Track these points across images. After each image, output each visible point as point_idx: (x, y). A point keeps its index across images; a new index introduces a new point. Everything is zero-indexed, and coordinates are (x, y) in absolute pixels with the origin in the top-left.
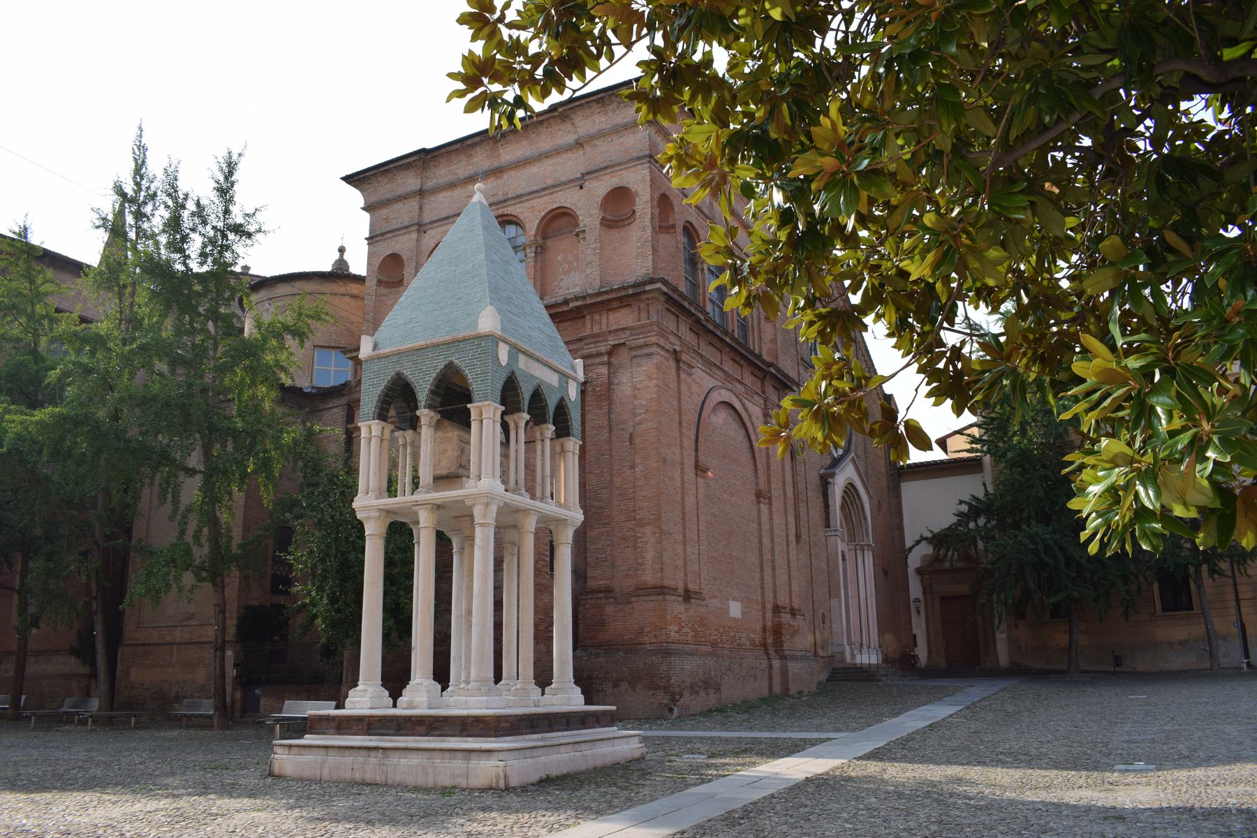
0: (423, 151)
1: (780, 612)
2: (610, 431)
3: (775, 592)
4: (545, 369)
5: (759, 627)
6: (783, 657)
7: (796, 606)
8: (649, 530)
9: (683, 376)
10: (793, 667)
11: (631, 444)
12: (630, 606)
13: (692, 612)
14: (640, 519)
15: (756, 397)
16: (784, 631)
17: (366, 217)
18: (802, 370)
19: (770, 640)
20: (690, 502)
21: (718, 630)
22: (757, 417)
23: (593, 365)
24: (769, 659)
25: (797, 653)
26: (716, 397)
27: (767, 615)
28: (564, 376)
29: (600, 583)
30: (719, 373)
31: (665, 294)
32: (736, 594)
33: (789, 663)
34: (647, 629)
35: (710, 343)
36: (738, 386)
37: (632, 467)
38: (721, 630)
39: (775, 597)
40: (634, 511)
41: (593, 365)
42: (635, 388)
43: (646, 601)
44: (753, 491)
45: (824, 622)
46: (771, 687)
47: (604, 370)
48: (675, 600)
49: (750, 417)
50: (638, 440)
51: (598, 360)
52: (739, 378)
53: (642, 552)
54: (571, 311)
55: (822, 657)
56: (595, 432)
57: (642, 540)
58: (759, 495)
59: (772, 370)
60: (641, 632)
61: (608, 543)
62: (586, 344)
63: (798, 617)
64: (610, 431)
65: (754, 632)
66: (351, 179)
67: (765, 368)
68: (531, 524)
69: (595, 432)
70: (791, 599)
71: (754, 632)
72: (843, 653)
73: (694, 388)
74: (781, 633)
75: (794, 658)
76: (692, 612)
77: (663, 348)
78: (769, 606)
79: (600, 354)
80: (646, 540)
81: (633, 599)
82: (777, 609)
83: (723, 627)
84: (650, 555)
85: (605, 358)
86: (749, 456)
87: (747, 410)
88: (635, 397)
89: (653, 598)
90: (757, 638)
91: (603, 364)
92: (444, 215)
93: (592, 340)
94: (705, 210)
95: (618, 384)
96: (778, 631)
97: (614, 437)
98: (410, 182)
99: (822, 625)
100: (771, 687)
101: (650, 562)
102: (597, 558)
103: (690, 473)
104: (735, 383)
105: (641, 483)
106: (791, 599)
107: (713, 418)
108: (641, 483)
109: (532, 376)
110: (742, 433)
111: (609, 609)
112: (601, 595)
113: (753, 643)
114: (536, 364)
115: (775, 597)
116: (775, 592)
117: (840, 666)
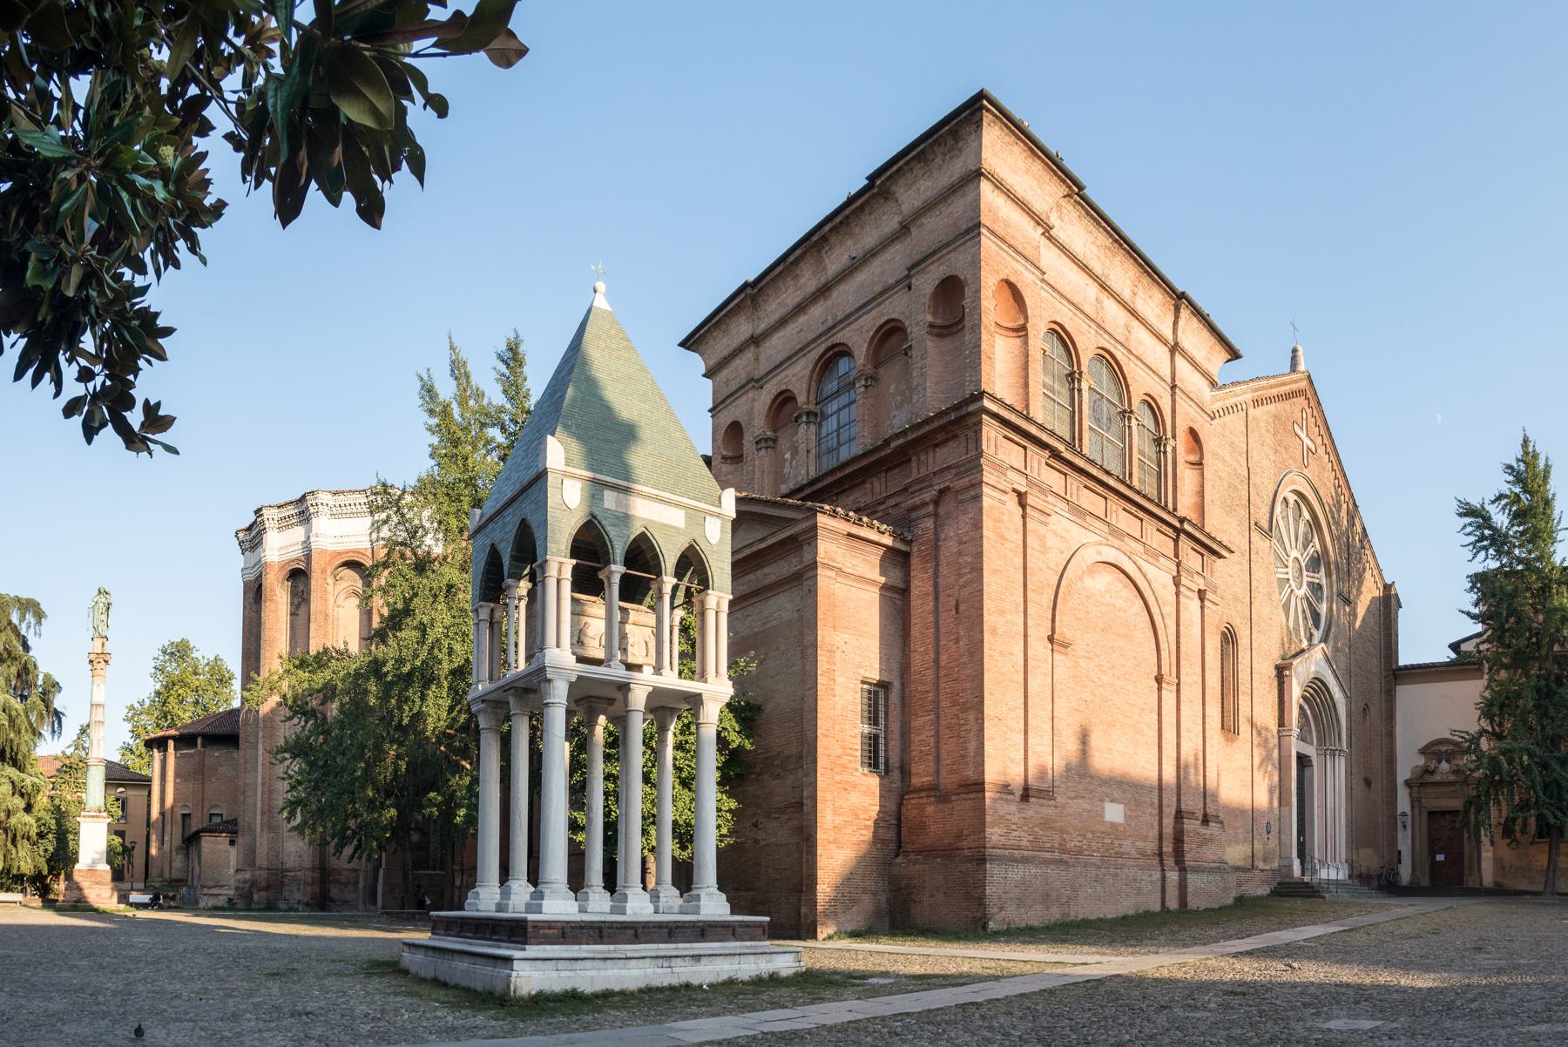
1: (1182, 818)
2: (937, 599)
3: (1179, 795)
5: (1154, 833)
6: (1183, 870)
7: (1211, 810)
8: (971, 716)
9: (1031, 525)
10: (1194, 880)
11: (957, 613)
12: (950, 805)
13: (1030, 813)
14: (964, 703)
16: (1186, 839)
19: (1168, 848)
20: (1038, 682)
23: (918, 518)
24: (1163, 870)
25: (1205, 864)
26: (1090, 555)
27: (1165, 821)
29: (924, 779)
30: (1098, 524)
33: (1189, 876)
34: (965, 833)
37: (957, 641)
38: (1089, 835)
39: (1179, 800)
40: (958, 695)
41: (918, 518)
42: (961, 543)
43: (965, 800)
45: (1268, 833)
46: (1163, 902)
47: (929, 523)
50: (962, 607)
51: (923, 512)
53: (965, 742)
54: (895, 453)
55: (1262, 871)
56: (920, 602)
57: (965, 727)
58: (1159, 679)
60: (959, 836)
61: (932, 733)
62: (912, 493)
63: (1211, 824)
64: (937, 599)
65: (1145, 839)
69: (920, 602)
70: (1205, 804)
72: (1290, 867)
73: (1051, 542)
74: (1183, 841)
75: (1196, 870)
76: (1030, 813)
78: (1170, 811)
79: (925, 504)
80: (968, 727)
81: (953, 798)
82: (1179, 815)
83: (1093, 832)
84: (972, 746)
85: (931, 508)
88: (960, 553)
89: (972, 796)
90: (1151, 846)
91: (928, 515)
92: (778, 362)
93: (917, 487)
95: (945, 540)
96: (1178, 840)
97: (940, 606)
99: (1265, 835)
100: (1163, 902)
101: (972, 754)
102: (921, 752)
103: (1039, 647)
105: (965, 659)
106: (1205, 804)
107: (1088, 581)
108: (965, 659)
111: (930, 810)
112: (923, 794)
113: (1143, 854)
115: (1179, 800)
116: (1179, 795)
117: (1287, 880)
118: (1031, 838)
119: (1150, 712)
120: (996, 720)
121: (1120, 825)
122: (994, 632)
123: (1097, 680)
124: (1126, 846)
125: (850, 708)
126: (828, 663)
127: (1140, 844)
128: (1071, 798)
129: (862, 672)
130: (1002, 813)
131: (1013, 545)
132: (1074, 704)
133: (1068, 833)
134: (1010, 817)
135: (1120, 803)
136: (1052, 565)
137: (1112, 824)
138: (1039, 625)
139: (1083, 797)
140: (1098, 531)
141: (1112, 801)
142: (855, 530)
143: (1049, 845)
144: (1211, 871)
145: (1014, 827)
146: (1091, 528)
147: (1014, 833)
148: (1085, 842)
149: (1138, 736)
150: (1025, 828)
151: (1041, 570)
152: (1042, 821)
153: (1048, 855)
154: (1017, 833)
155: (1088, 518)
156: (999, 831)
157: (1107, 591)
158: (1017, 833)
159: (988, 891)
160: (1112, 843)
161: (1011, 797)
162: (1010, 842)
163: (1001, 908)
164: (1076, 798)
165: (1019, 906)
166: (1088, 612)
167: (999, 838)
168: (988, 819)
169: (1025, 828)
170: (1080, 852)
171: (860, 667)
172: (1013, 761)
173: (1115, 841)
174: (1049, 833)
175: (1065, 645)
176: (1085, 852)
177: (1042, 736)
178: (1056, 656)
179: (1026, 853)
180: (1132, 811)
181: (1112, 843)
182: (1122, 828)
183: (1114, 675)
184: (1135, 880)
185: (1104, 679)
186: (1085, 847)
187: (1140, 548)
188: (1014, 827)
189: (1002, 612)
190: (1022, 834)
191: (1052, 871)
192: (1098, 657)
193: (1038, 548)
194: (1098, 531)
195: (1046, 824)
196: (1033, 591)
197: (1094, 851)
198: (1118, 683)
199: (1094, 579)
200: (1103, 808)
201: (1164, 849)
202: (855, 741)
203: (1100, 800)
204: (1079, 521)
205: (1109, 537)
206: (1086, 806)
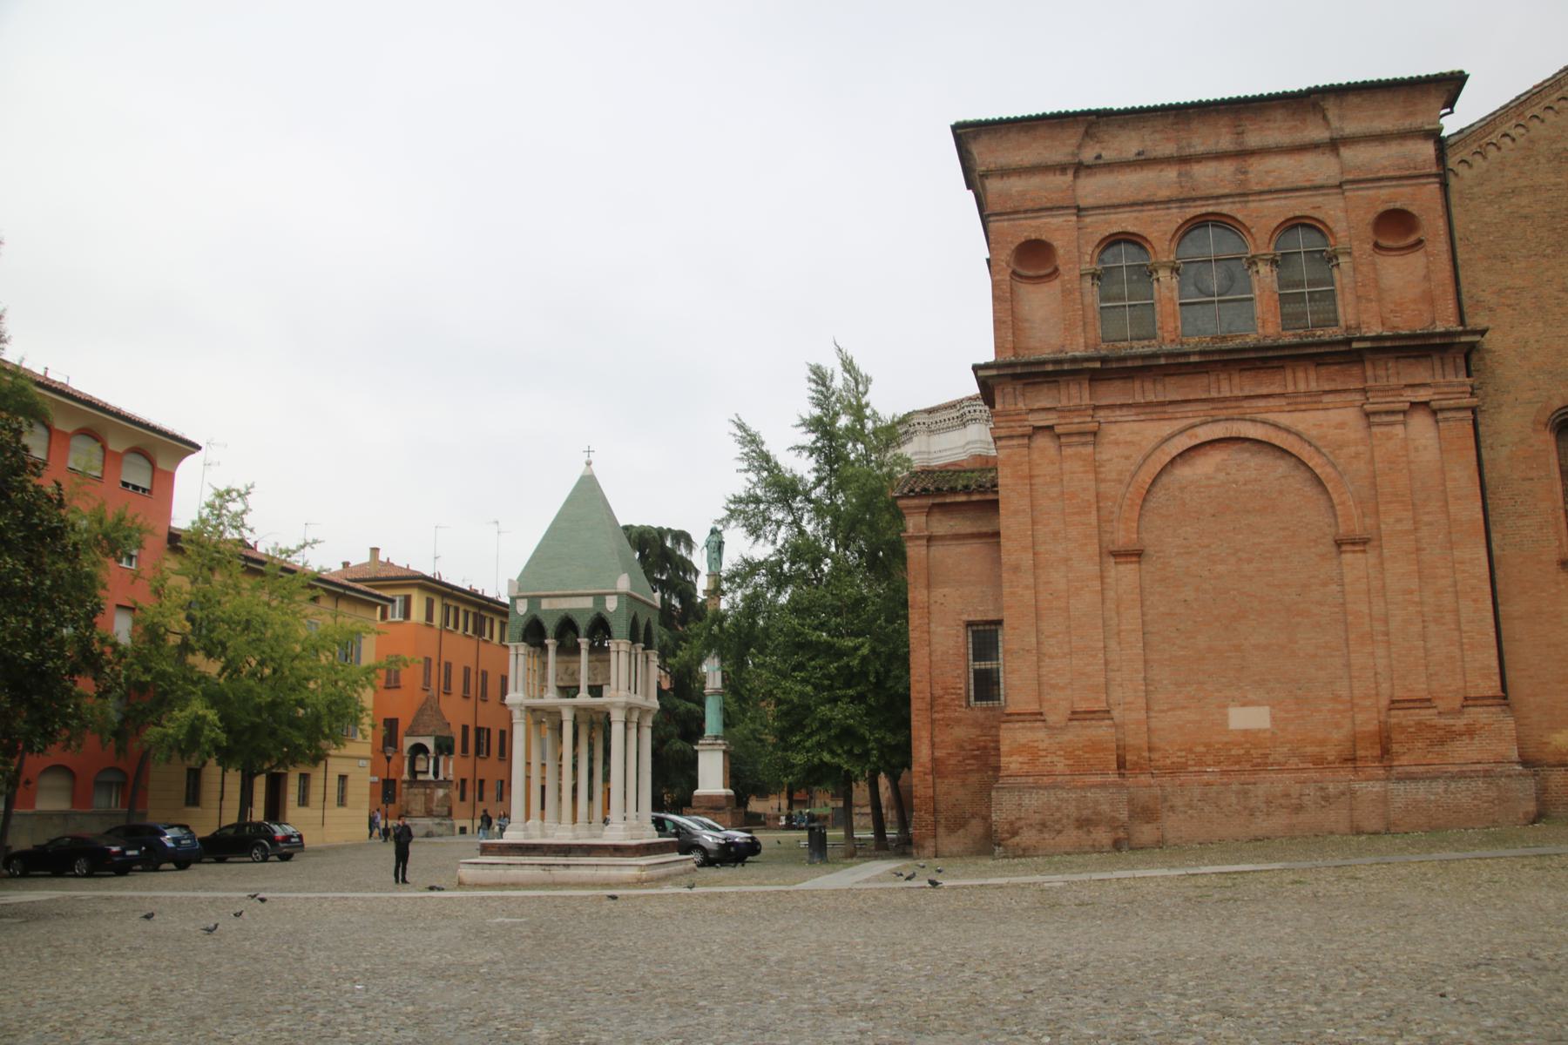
4: (573, 599)
15: (1327, 399)
21: (1190, 751)
22: (1341, 425)
25: (1450, 768)
28: (600, 598)
31: (999, 376)
32: (1251, 696)
35: (1166, 375)
36: (1261, 403)
44: (1329, 540)
48: (1023, 728)
49: (1298, 435)
52: (1278, 391)
58: (1339, 544)
59: (1355, 345)
67: (1342, 348)
71: (1322, 743)
77: (1011, 437)
86: (1310, 491)
87: (1288, 430)
94: (1164, 194)
107: (1184, 472)
110: (1282, 466)
114: (562, 600)
118: (1071, 762)
119: (1324, 584)
120: (1021, 652)
121: (1265, 731)
125: (951, 652)
126: (919, 619)
127: (1310, 749)
128: (1162, 711)
129: (965, 617)
130: (1023, 741)
131: (1048, 479)
132: (1162, 609)
134: (1036, 744)
135: (1263, 705)
136: (1114, 475)
137: (1246, 732)
138: (1086, 544)
139: (1184, 708)
140: (1190, 415)
141: (1244, 705)
143: (1101, 767)
144: (1462, 775)
145: (1044, 753)
146: (1179, 415)
147: (1042, 760)
149: (1299, 619)
150: (1062, 753)
151: (1084, 490)
152: (1090, 743)
153: (1098, 779)
154: (1048, 759)
155: (1170, 409)
156: (1020, 759)
157: (1218, 470)
158: (1048, 759)
159: (994, 819)
160: (1248, 753)
162: (1037, 769)
163: (1015, 833)
164: (1169, 710)
167: (1018, 766)
168: (1004, 748)
169: (1062, 753)
171: (962, 613)
172: (1053, 687)
173: (1252, 751)
174: (1101, 755)
176: (1190, 769)
179: (1060, 778)
181: (1248, 753)
182: (1268, 735)
184: (1287, 795)
185: (1221, 568)
186: (1190, 763)
188: (1044, 753)
190: (1056, 759)
191: (1100, 795)
193: (1082, 469)
194: (1190, 415)
195: (1095, 746)
196: (1074, 514)
197: (1209, 766)
200: (1226, 715)
202: (958, 680)
205: (1216, 412)
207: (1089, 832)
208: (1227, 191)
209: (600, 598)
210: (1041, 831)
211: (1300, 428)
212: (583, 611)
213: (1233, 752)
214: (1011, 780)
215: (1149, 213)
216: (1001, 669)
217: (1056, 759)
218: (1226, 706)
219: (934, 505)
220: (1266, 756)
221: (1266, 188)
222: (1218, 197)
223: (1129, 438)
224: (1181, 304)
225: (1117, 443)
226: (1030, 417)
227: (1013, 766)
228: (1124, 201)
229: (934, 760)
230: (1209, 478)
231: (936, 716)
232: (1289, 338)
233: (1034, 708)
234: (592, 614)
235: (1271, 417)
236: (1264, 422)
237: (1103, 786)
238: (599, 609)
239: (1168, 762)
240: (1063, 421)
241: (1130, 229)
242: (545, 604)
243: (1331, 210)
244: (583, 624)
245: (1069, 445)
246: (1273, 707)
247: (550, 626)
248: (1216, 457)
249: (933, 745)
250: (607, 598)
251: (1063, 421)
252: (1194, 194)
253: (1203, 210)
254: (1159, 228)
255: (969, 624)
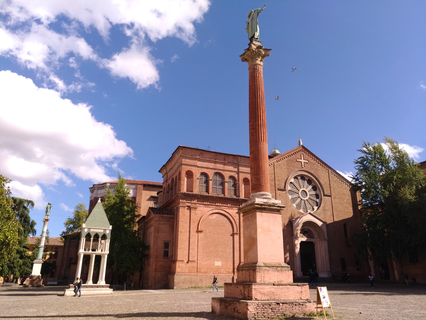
0: (164, 165)
5: (232, 268)
9: (192, 211)
15: (234, 208)
17: (163, 178)
18: (278, 192)
26: (211, 212)
36: (224, 207)
66: (159, 172)
68: (94, 256)
71: (229, 269)
83: (211, 268)
98: (165, 171)
104: (221, 207)
107: (211, 217)
109: (95, 232)
114: (96, 229)
122: (181, 232)
123: (213, 236)
124: (222, 271)
127: (228, 270)
129: (164, 240)
130: (180, 266)
132: (205, 242)
133: (202, 269)
136: (199, 217)
137: (217, 266)
142: (162, 215)
147: (184, 270)
148: (208, 270)
149: (227, 246)
151: (194, 218)
153: (193, 274)
154: (185, 270)
157: (216, 218)
158: (185, 270)
161: (183, 262)
163: (178, 284)
164: (205, 261)
165: (183, 284)
166: (210, 223)
168: (177, 267)
170: (206, 272)
175: (201, 232)
177: (194, 250)
178: (199, 234)
180: (224, 263)
183: (218, 234)
185: (215, 236)
187: (227, 207)
189: (183, 228)
190: (186, 270)
192: (213, 232)
195: (193, 267)
198: (220, 236)
199: (212, 216)
201: (235, 271)
203: (213, 261)
204: (207, 207)
205: (216, 208)
206: (209, 263)
207: (191, 284)
208: (221, 169)
209: (105, 230)
210: (183, 284)
211: (229, 212)
212: (101, 232)
213: (215, 270)
214: (178, 273)
215: (209, 170)
216: (169, 250)
217: (186, 270)
218: (214, 261)
219: (161, 217)
220: (220, 271)
221: (227, 170)
222: (220, 170)
223: (202, 210)
224: (212, 187)
225: (200, 211)
226: (186, 203)
227: (178, 270)
228: (205, 167)
229: (156, 269)
230: (214, 219)
231: (157, 259)
232: (229, 197)
233: (182, 259)
234: (103, 234)
235: (225, 210)
236: (224, 211)
237: (194, 275)
238: (104, 233)
239: (204, 271)
240: (192, 205)
241: (205, 172)
242: (92, 230)
243: (236, 176)
244: (100, 236)
245: (192, 210)
246: (222, 262)
247: (93, 235)
248: (217, 215)
249: (156, 265)
250: (107, 230)
251: (192, 205)
252: (216, 168)
253: (217, 171)
254: (211, 174)
255: (165, 241)
